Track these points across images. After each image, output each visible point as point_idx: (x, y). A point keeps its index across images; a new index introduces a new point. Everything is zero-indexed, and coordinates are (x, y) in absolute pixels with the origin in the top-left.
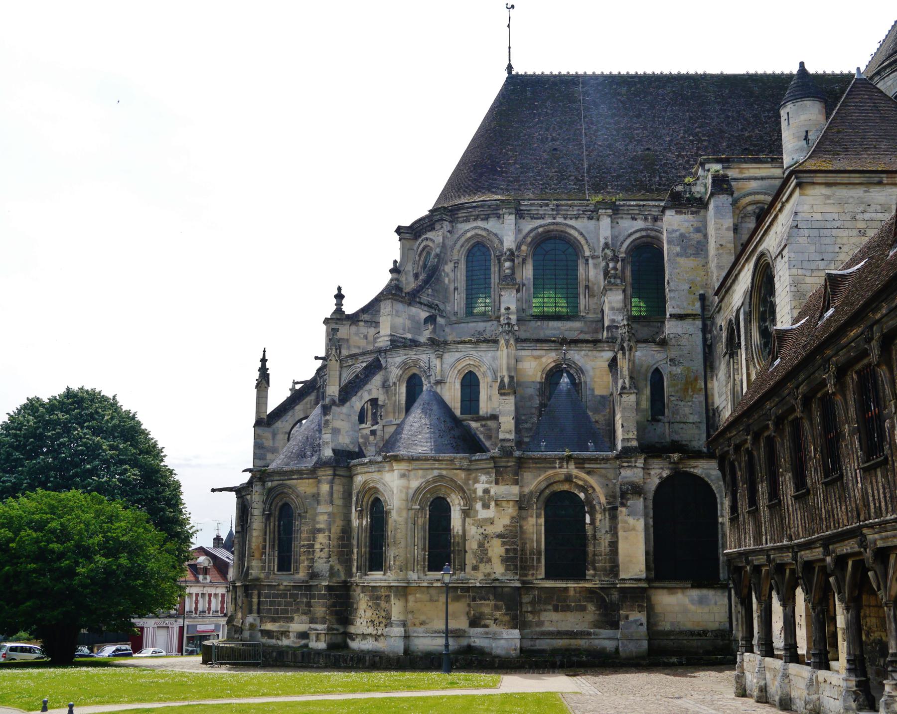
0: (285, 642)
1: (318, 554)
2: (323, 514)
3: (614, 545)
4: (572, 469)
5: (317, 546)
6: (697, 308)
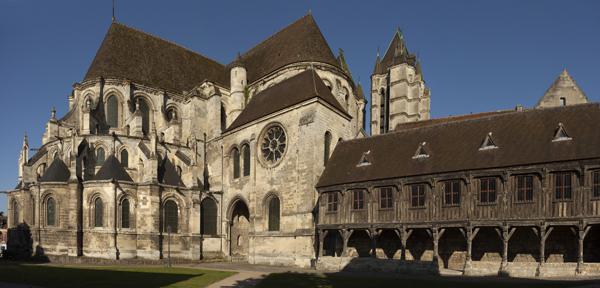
0: (54, 253)
1: (70, 219)
2: (73, 204)
3: (188, 221)
4: (175, 192)
5: (70, 216)
6: (202, 138)
